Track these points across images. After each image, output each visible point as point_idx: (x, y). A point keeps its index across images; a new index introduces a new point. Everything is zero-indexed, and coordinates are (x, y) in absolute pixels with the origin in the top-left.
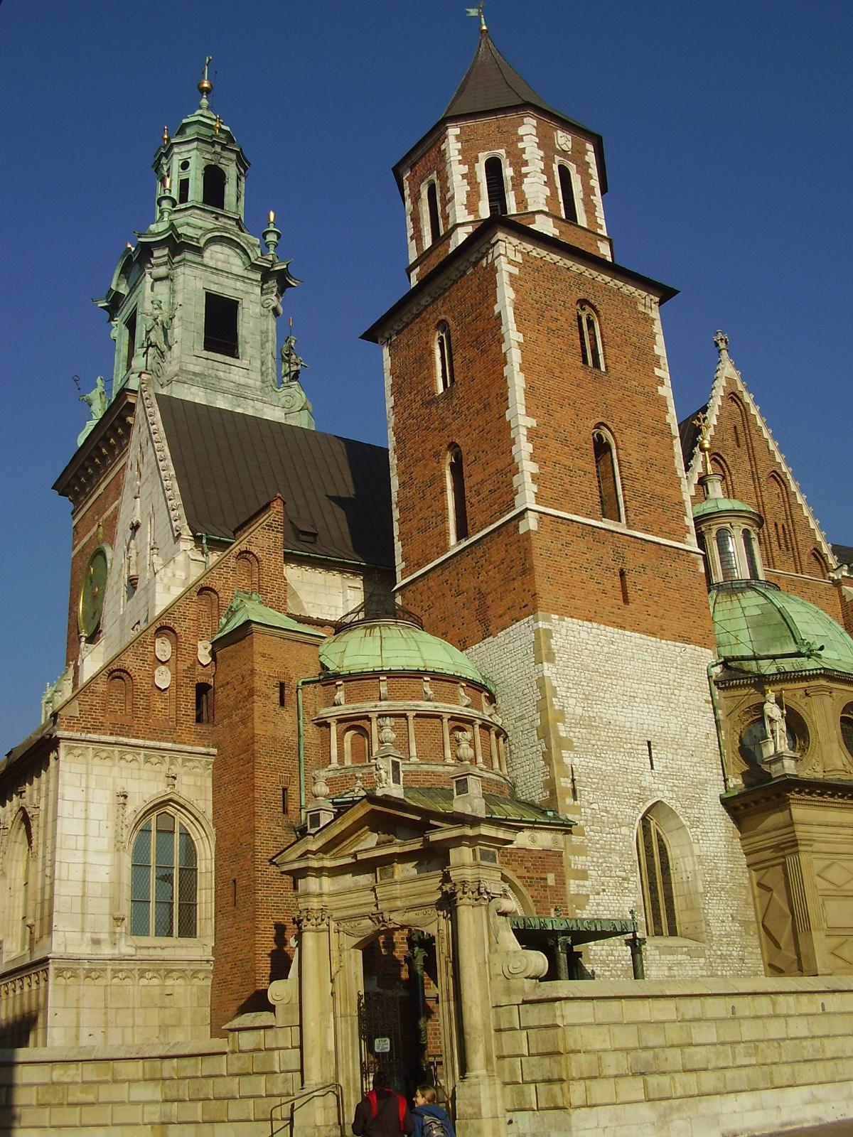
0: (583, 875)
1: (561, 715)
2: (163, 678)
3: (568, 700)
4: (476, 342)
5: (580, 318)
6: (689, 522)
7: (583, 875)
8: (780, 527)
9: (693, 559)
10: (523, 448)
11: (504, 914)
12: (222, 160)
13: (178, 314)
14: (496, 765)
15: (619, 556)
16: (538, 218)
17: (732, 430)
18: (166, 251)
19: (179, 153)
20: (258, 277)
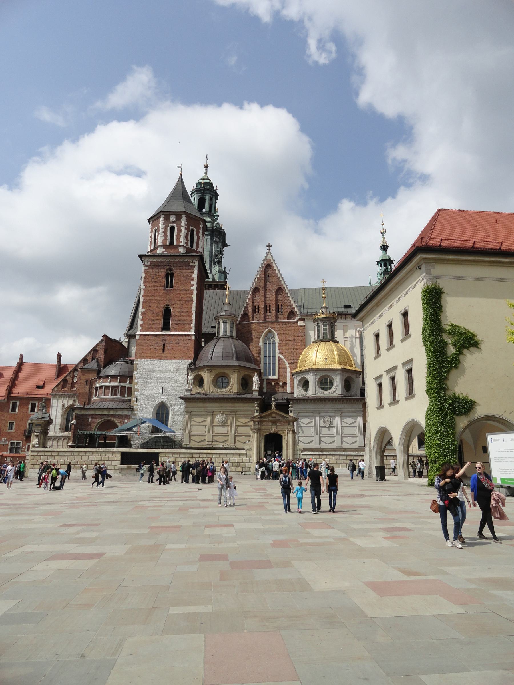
1: (137, 384)
6: (193, 325)
9: (191, 336)
15: (164, 340)
19: (193, 196)
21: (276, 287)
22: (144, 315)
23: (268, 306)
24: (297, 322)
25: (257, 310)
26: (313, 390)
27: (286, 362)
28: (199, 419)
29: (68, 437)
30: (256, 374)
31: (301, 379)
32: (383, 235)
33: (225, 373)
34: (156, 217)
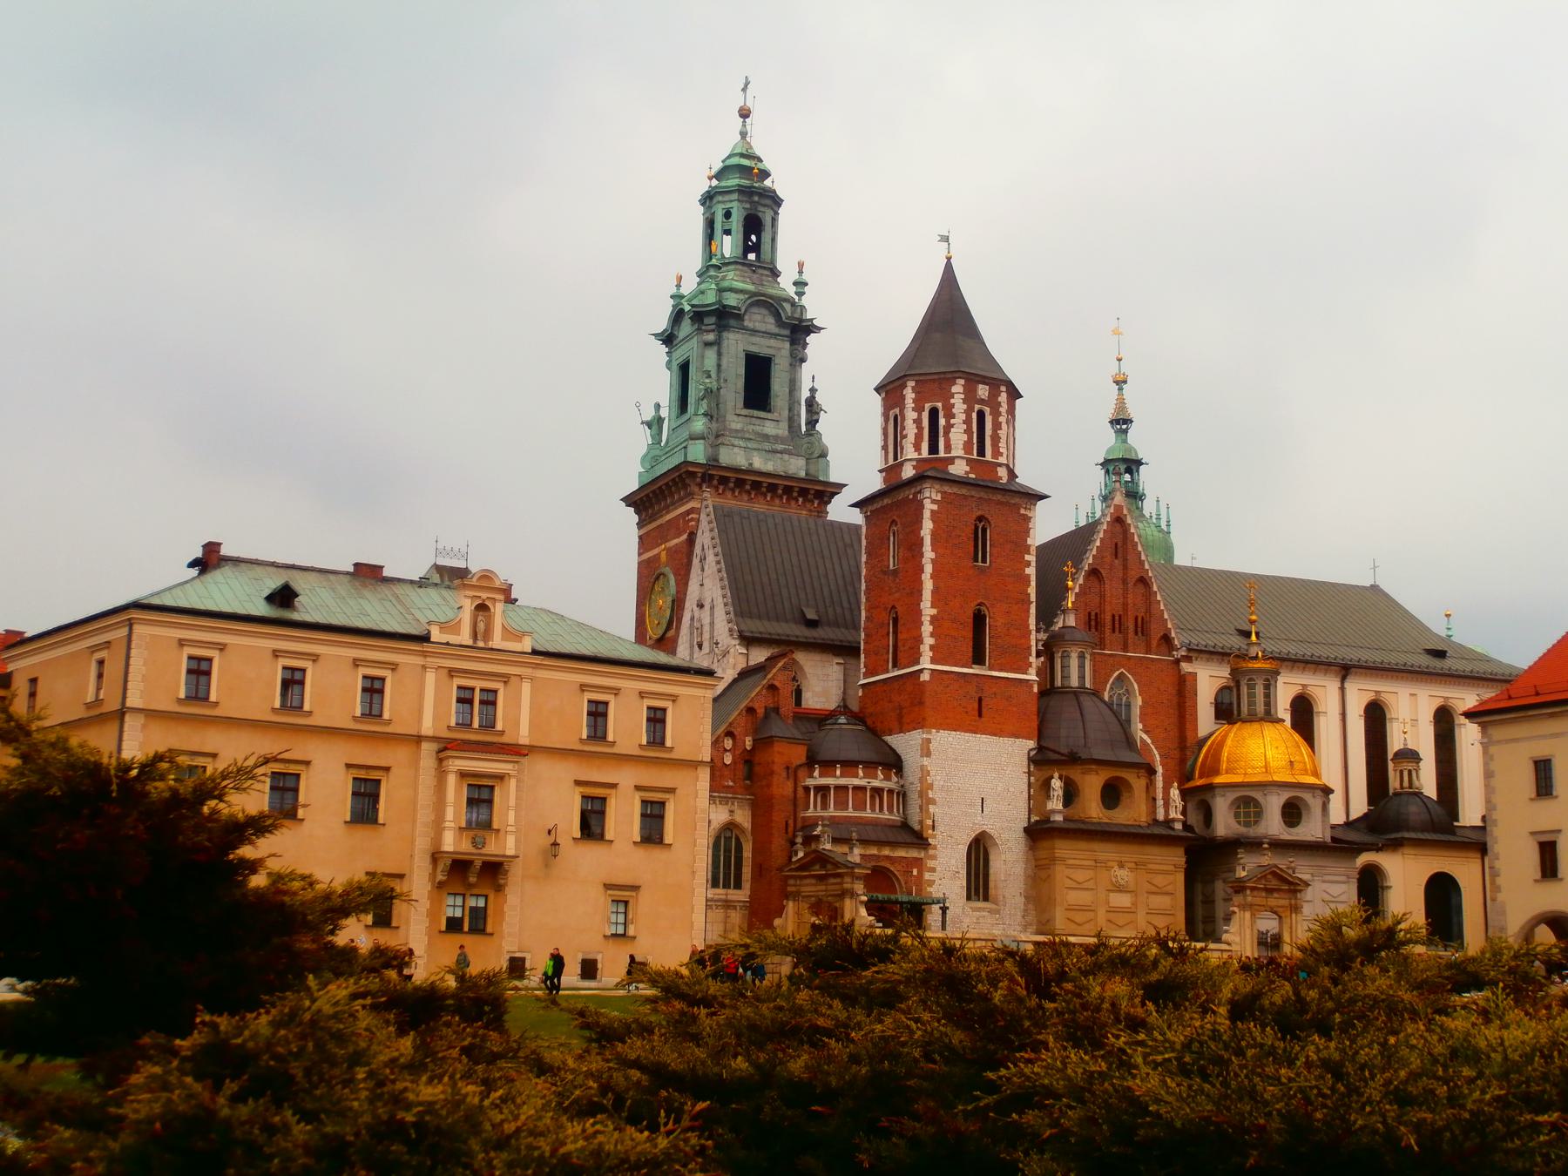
0: (933, 870)
1: (931, 787)
2: (728, 759)
3: (937, 778)
4: (910, 548)
5: (976, 528)
6: (1032, 659)
7: (933, 870)
8: (1140, 620)
10: (927, 628)
11: (862, 902)
12: (762, 209)
13: (723, 375)
14: (895, 810)
16: (957, 461)
17: (1114, 547)
18: (711, 320)
19: (723, 202)
20: (787, 332)
21: (1134, 574)
22: (936, 623)
23: (1117, 618)
24: (1177, 662)
25: (1093, 623)
26: (1273, 825)
27: (1156, 752)
28: (1080, 875)
29: (726, 901)
30: (1176, 784)
31: (1237, 799)
32: (1119, 389)
33: (1122, 778)
34: (936, 377)
